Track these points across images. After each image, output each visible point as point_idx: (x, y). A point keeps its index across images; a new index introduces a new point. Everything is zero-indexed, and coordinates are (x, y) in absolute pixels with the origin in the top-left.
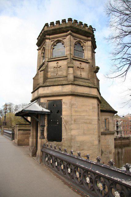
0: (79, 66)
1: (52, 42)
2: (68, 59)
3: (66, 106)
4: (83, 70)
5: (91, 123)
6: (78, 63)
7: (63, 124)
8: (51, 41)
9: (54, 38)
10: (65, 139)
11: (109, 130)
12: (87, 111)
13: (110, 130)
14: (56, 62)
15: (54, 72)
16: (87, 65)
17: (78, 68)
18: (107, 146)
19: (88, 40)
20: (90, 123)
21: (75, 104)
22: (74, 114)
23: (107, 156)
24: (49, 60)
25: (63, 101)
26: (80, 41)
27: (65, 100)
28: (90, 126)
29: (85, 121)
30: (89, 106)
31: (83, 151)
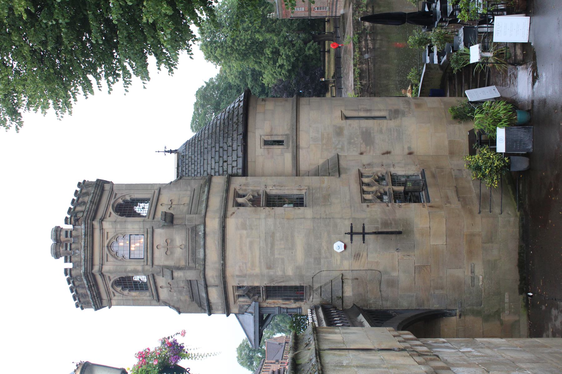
0: (163, 251)
1: (116, 294)
2: (153, 275)
3: (243, 281)
4: (169, 241)
5: (273, 233)
6: (157, 253)
7: (276, 285)
8: (115, 296)
9: (108, 293)
10: (302, 283)
11: (286, 135)
12: (251, 243)
13: (287, 132)
14: (160, 290)
15: (180, 292)
16: (158, 231)
17: (169, 253)
18: (324, 142)
19: (102, 229)
20: (273, 235)
21: (240, 267)
22: (257, 271)
23: (346, 143)
24: (155, 297)
25: (236, 284)
26: (107, 247)
27: (232, 282)
28: (278, 235)
29: (270, 245)
30: (241, 237)
31: (323, 251)
